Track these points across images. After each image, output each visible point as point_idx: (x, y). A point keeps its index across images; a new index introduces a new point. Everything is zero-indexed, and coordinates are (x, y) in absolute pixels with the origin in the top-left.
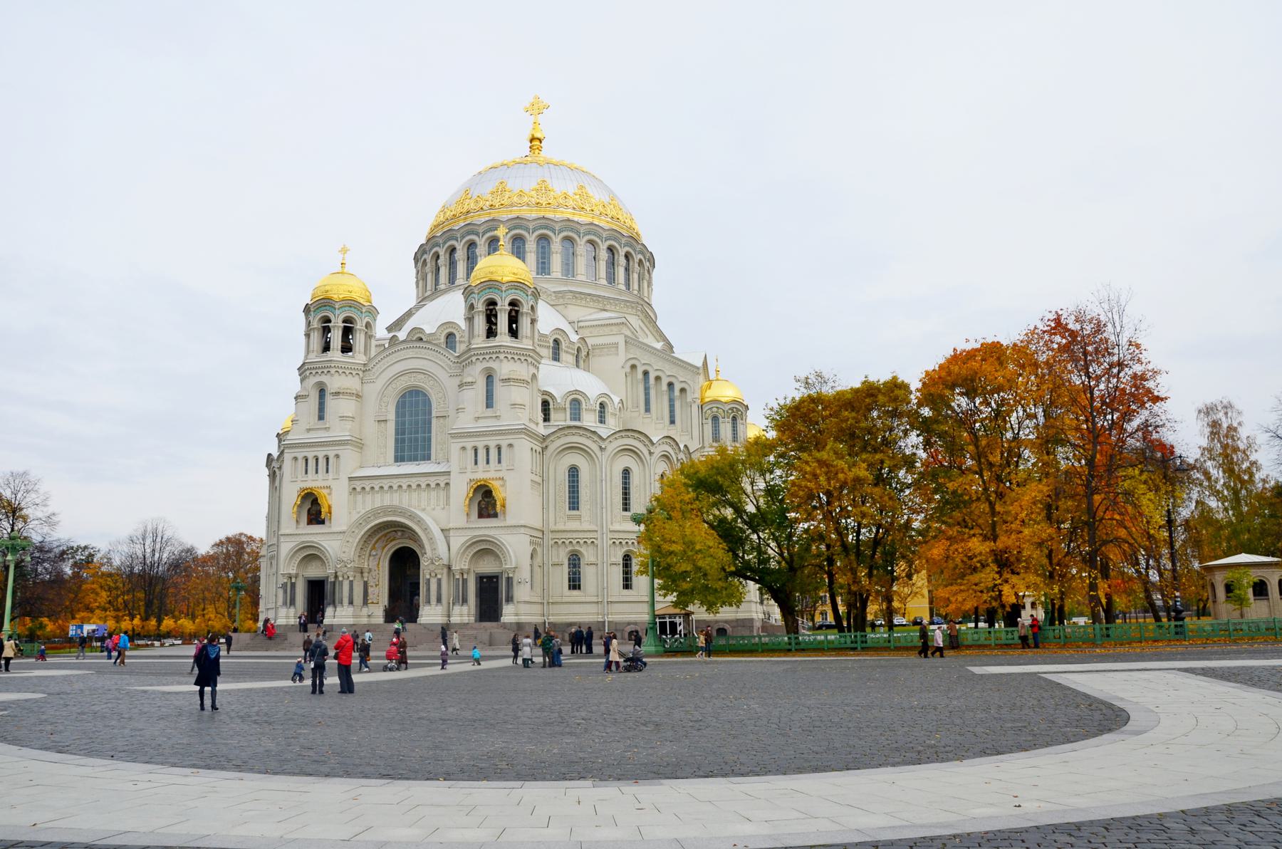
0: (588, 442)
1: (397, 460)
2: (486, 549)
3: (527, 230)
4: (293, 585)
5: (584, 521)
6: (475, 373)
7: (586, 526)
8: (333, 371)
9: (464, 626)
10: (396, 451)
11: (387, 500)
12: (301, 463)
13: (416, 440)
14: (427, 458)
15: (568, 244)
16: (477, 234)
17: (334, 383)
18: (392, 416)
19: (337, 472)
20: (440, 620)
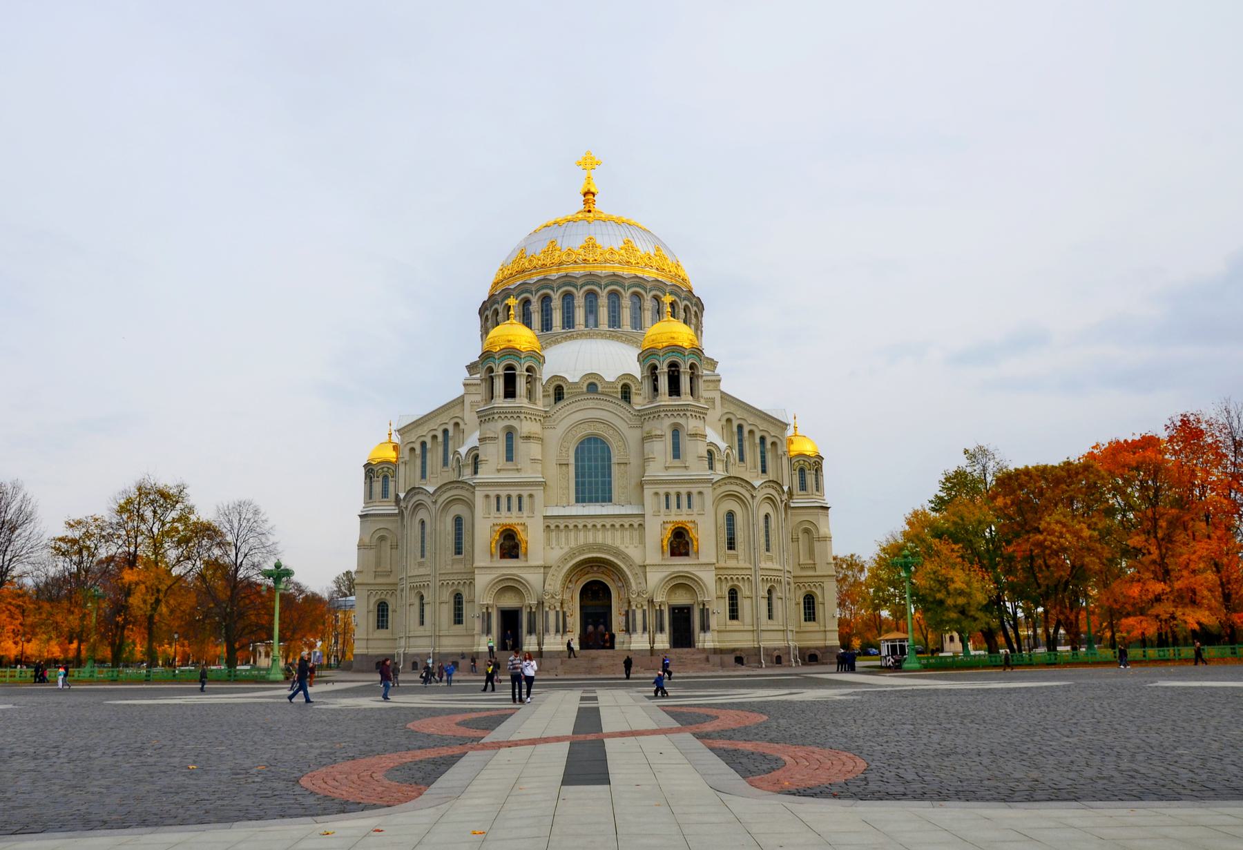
0: (743, 491)
1: (577, 501)
2: (682, 583)
3: (623, 286)
4: (489, 615)
5: (739, 561)
6: (663, 426)
7: (742, 564)
8: (522, 416)
9: (664, 651)
10: (577, 492)
11: (584, 538)
12: (494, 501)
13: (597, 483)
14: (607, 499)
15: (636, 300)
16: (575, 286)
17: (526, 427)
18: (572, 461)
19: (532, 510)
20: (648, 646)
